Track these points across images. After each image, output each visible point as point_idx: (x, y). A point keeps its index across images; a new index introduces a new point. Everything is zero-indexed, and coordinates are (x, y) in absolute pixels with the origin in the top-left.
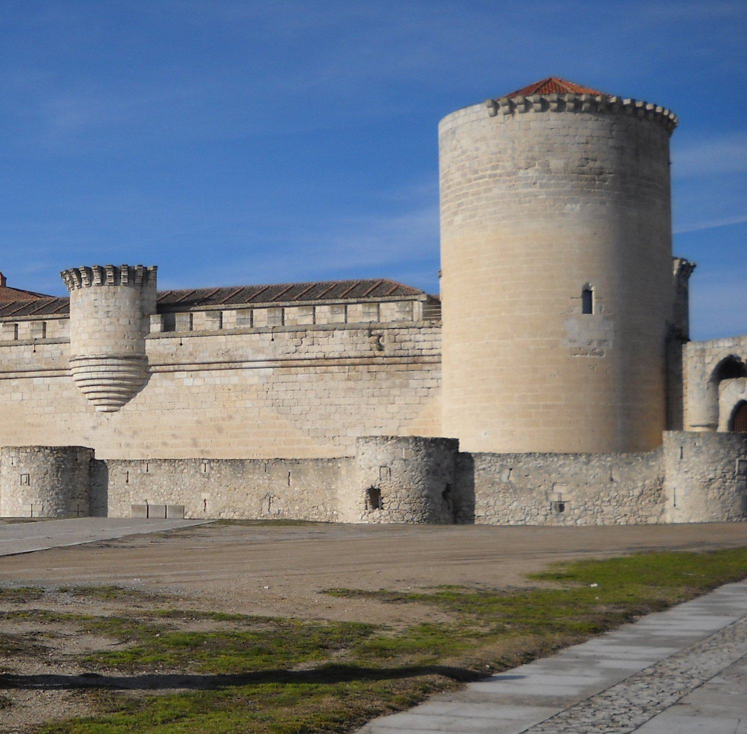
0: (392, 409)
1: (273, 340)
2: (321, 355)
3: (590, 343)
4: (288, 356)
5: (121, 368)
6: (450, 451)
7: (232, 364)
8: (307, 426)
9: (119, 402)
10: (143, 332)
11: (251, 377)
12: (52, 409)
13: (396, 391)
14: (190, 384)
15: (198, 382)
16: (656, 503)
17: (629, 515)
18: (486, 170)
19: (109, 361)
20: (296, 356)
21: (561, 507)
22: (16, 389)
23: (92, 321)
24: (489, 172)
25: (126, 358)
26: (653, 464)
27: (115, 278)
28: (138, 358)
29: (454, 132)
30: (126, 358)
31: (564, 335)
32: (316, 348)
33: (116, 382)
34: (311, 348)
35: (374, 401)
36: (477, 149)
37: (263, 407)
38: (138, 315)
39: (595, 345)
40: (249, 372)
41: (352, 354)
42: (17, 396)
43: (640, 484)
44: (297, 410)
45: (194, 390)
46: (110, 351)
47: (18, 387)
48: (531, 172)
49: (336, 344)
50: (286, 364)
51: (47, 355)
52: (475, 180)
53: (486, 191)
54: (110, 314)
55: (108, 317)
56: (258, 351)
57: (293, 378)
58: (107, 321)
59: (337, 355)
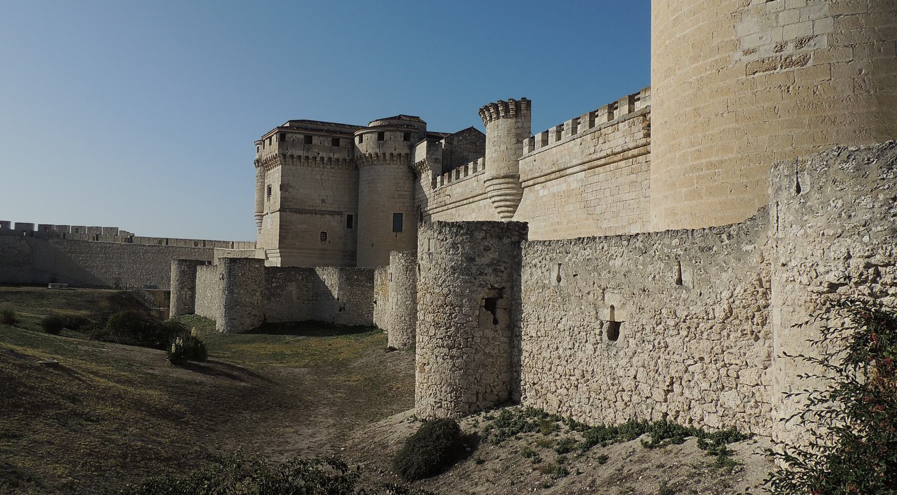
3: (781, 48)
5: (502, 186)
6: (500, 238)
7: (561, 172)
9: (509, 214)
10: (518, 153)
11: (573, 182)
15: (546, 192)
16: (757, 339)
17: (707, 360)
19: (495, 181)
20: (594, 157)
21: (614, 330)
25: (504, 177)
26: (750, 247)
27: (506, 113)
28: (512, 177)
30: (504, 177)
31: (736, 44)
33: (502, 198)
38: (514, 140)
39: (790, 49)
40: (571, 177)
41: (631, 145)
43: (726, 294)
46: (502, 172)
50: (590, 165)
57: (596, 178)
59: (620, 150)
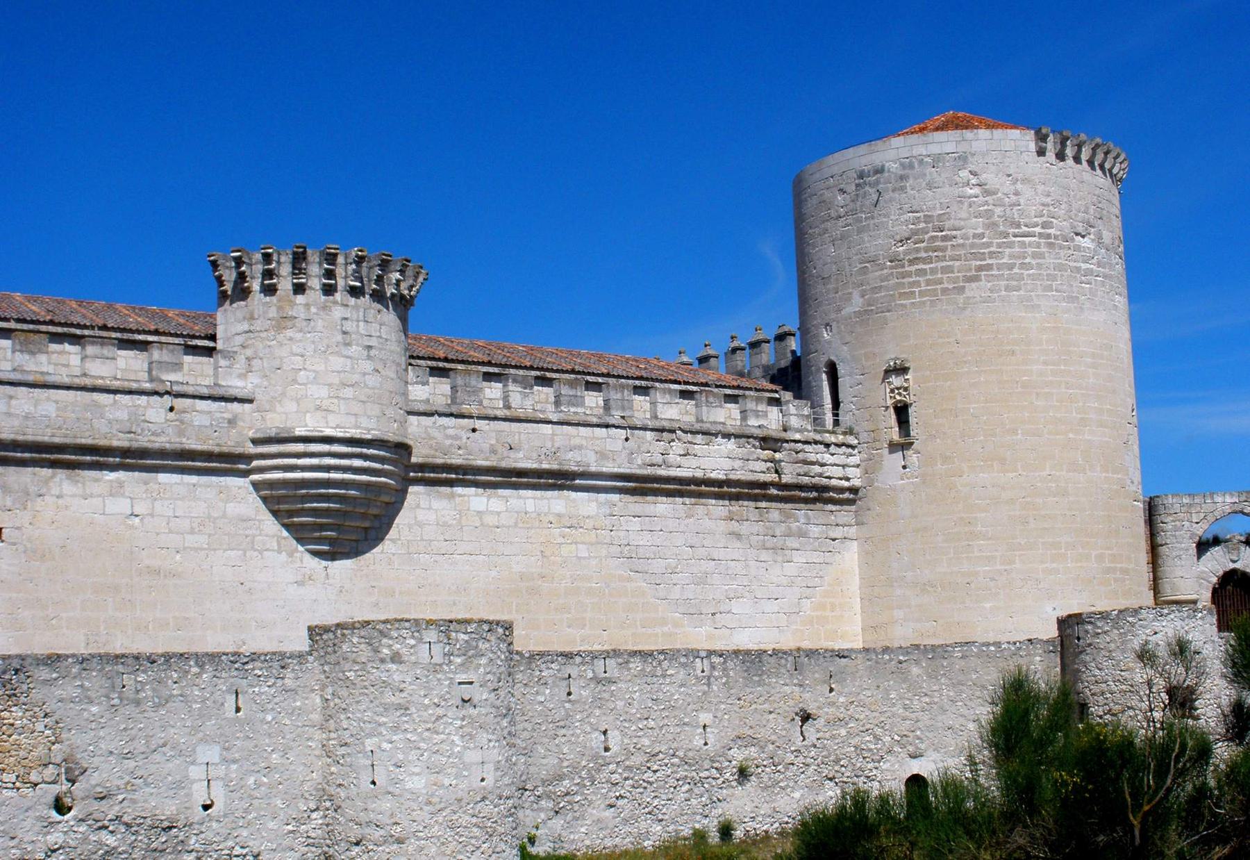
0: (790, 569)
1: (627, 439)
2: (699, 474)
4: (649, 471)
8: (676, 593)
12: (201, 540)
13: (792, 542)
14: (482, 508)
18: (1036, 225)
22: (116, 491)
23: (337, 362)
24: (1038, 230)
29: (963, 159)
32: (690, 462)
34: (684, 461)
35: (764, 555)
36: (1017, 193)
37: (606, 557)
42: (120, 506)
44: (658, 565)
45: (490, 520)
47: (121, 484)
48: (1086, 243)
49: (718, 459)
51: (198, 420)
52: (1015, 236)
53: (1035, 255)
54: (373, 352)
55: (369, 357)
56: (602, 455)
58: (368, 366)
